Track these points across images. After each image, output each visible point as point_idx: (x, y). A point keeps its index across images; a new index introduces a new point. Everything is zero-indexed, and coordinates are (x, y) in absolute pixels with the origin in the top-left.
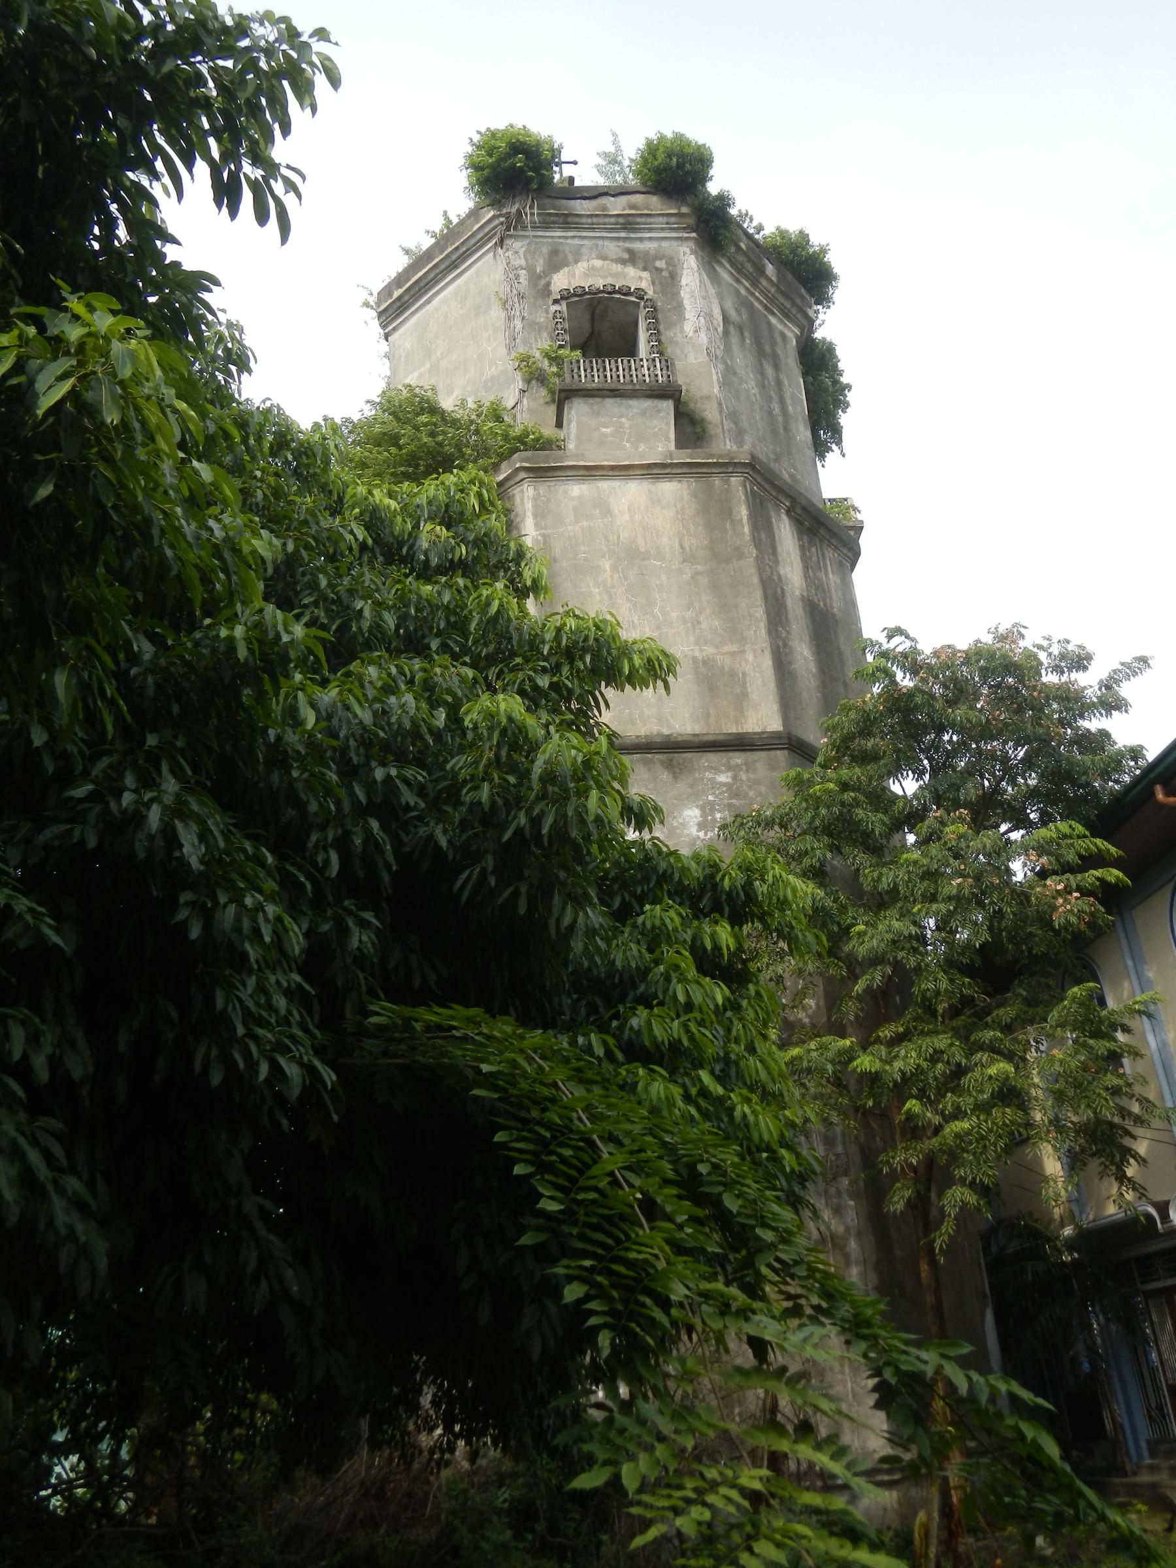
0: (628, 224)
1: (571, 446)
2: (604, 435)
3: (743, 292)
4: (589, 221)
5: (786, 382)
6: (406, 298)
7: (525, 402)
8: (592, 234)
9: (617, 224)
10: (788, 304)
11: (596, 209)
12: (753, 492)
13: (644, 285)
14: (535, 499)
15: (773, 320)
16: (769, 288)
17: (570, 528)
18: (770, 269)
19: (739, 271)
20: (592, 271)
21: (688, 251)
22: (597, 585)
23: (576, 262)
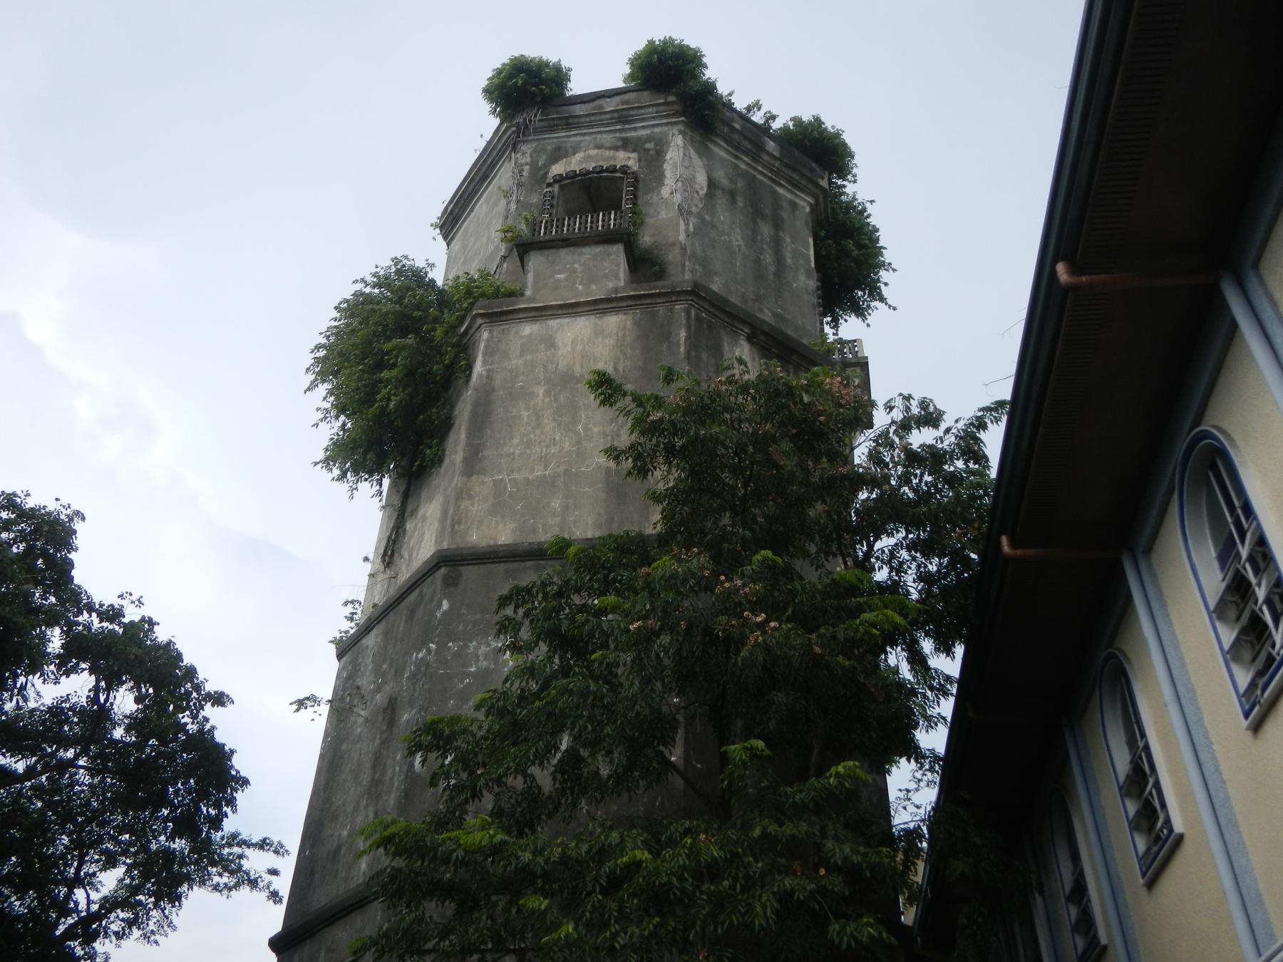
0: (623, 118)
1: (528, 293)
2: (559, 281)
3: (743, 166)
4: (588, 119)
5: (788, 239)
6: (457, 210)
7: (505, 266)
8: (591, 130)
9: (612, 119)
10: (795, 176)
11: (594, 109)
12: (699, 319)
13: (630, 163)
14: (488, 341)
15: (780, 190)
16: (773, 162)
17: (514, 362)
18: (771, 145)
19: (737, 148)
20: (588, 159)
21: (676, 132)
22: (527, 408)
23: (574, 153)
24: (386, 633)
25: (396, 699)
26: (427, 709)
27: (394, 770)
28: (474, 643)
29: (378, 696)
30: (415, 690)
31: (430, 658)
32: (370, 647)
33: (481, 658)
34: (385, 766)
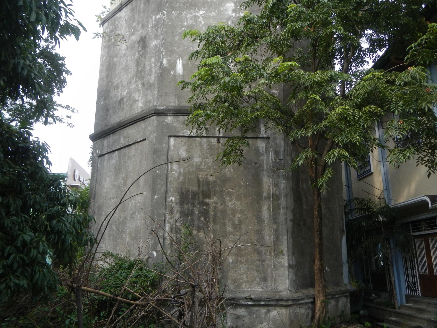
24: (132, 10)
25: (145, 37)
26: (166, 40)
27: (151, 66)
28: (185, 12)
29: (133, 37)
30: (157, 32)
31: (165, 17)
32: (123, 17)
33: (189, 19)
34: (144, 65)
